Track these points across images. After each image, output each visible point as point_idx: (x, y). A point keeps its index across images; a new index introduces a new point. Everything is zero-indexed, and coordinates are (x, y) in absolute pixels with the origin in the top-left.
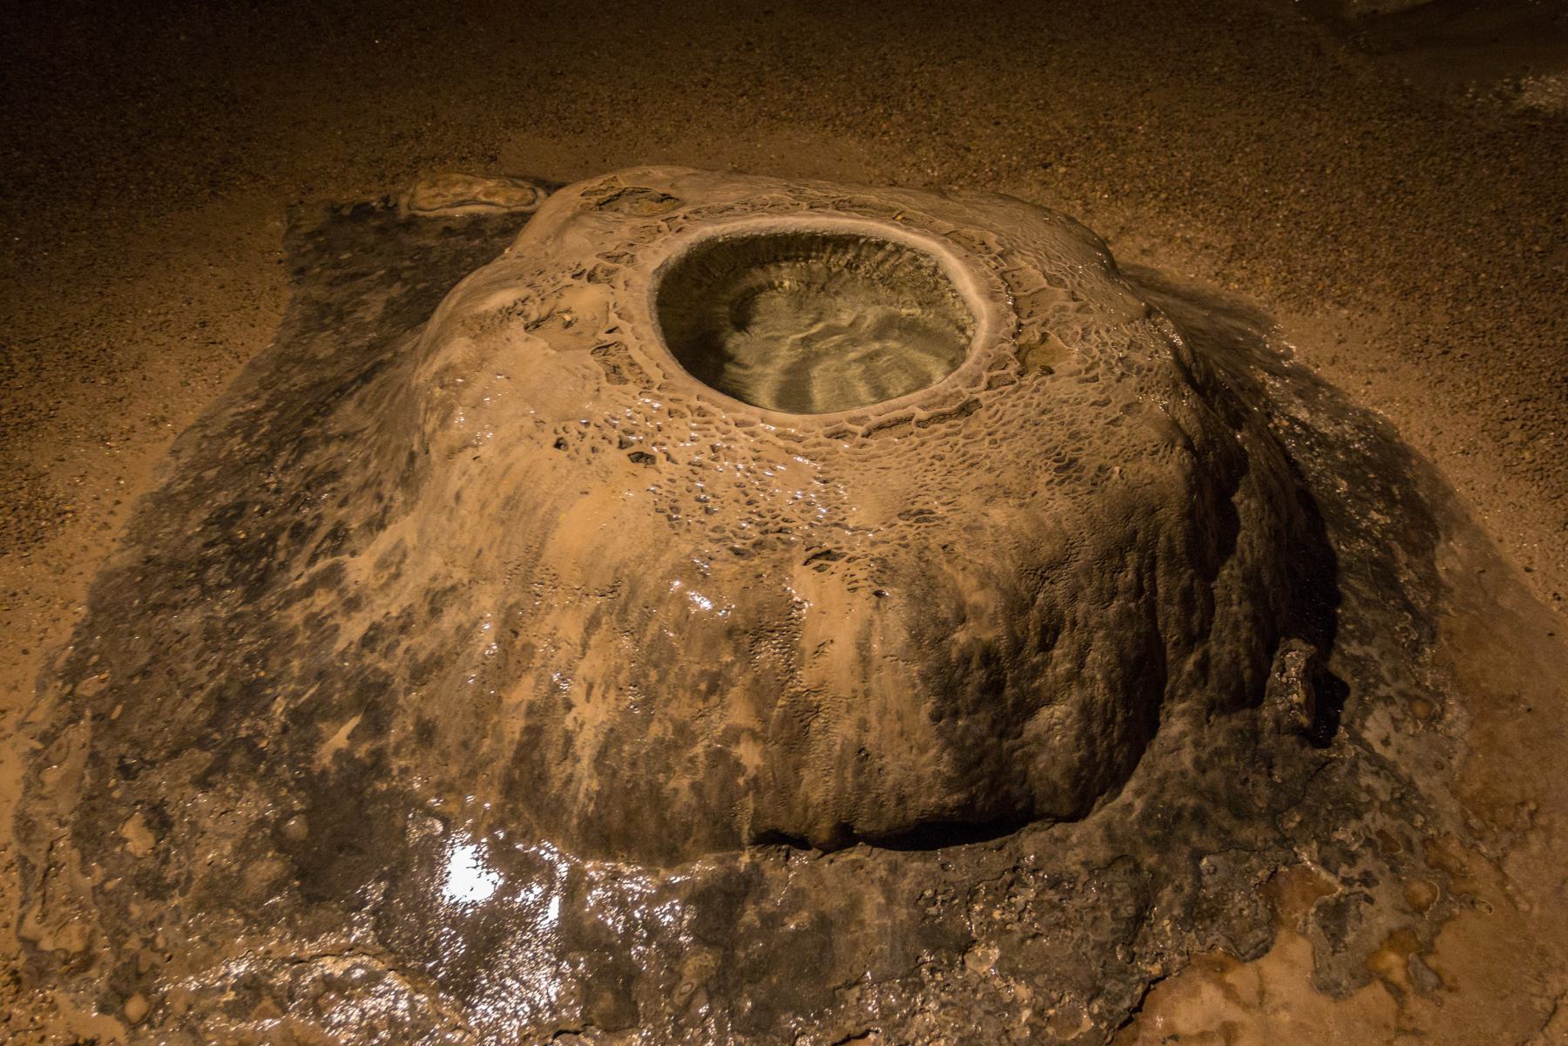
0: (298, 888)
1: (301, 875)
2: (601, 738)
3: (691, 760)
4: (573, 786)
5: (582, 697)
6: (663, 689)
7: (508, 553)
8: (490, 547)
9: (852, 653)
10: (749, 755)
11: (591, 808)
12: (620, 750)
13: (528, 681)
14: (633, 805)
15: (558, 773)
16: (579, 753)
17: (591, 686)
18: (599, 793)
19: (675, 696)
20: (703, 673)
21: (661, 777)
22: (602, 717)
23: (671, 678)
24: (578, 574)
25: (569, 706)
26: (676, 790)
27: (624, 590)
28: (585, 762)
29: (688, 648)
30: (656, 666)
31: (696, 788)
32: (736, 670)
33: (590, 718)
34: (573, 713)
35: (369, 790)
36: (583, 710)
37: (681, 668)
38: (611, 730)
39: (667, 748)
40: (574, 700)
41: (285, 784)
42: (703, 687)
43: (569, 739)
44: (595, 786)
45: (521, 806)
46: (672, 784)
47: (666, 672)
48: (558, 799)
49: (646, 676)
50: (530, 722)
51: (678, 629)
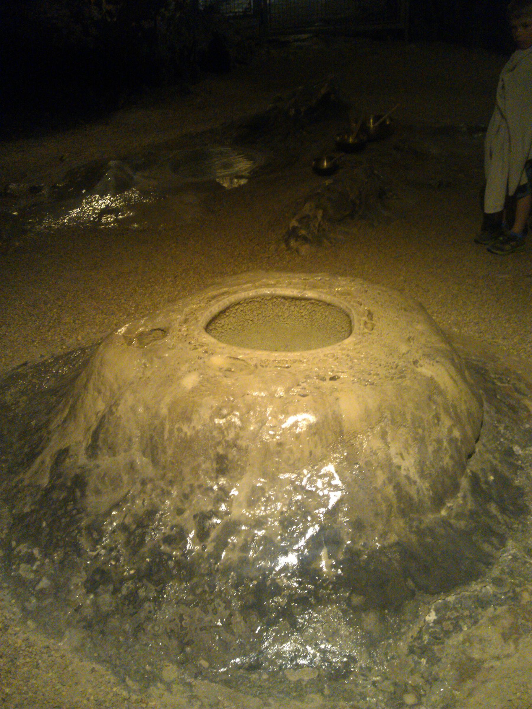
0: (389, 612)
1: (384, 608)
2: (418, 467)
3: (446, 449)
4: (421, 492)
5: (402, 461)
6: (426, 432)
7: (327, 441)
8: (316, 447)
9: (452, 382)
10: (456, 433)
11: (431, 493)
12: (427, 465)
13: (379, 473)
14: (441, 480)
15: (413, 492)
16: (414, 479)
17: (401, 454)
18: (431, 486)
19: (431, 432)
20: (433, 417)
21: (441, 463)
22: (413, 461)
23: (427, 427)
24: (364, 424)
25: (399, 467)
26: (447, 463)
27: (387, 414)
28: (418, 480)
29: (424, 413)
30: (419, 427)
31: (452, 457)
32: (438, 409)
33: (408, 465)
34: (402, 468)
35: (362, 563)
36: (405, 464)
37: (427, 421)
38: (420, 461)
39: (437, 451)
40: (399, 464)
41: (330, 594)
42: (436, 421)
43: (408, 477)
44: (427, 485)
45: (411, 515)
46: (445, 463)
47: (424, 426)
48: (420, 500)
49: (418, 434)
50: (394, 484)
51: (417, 409)
